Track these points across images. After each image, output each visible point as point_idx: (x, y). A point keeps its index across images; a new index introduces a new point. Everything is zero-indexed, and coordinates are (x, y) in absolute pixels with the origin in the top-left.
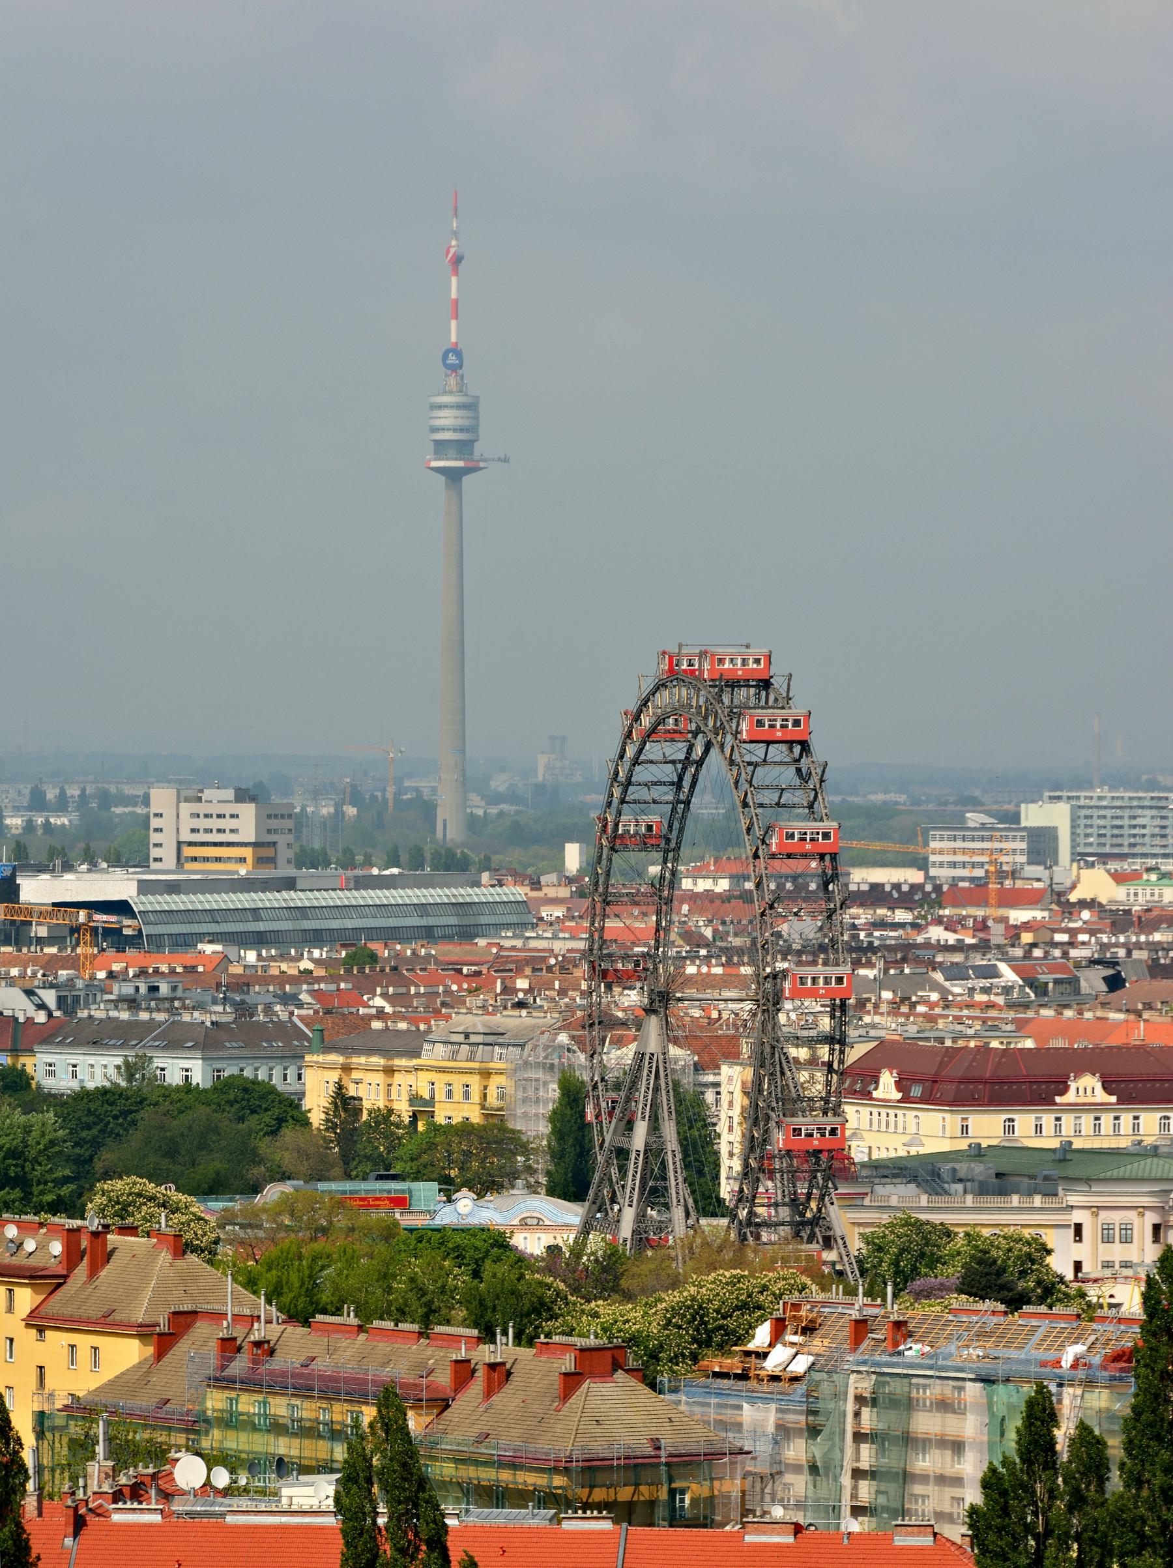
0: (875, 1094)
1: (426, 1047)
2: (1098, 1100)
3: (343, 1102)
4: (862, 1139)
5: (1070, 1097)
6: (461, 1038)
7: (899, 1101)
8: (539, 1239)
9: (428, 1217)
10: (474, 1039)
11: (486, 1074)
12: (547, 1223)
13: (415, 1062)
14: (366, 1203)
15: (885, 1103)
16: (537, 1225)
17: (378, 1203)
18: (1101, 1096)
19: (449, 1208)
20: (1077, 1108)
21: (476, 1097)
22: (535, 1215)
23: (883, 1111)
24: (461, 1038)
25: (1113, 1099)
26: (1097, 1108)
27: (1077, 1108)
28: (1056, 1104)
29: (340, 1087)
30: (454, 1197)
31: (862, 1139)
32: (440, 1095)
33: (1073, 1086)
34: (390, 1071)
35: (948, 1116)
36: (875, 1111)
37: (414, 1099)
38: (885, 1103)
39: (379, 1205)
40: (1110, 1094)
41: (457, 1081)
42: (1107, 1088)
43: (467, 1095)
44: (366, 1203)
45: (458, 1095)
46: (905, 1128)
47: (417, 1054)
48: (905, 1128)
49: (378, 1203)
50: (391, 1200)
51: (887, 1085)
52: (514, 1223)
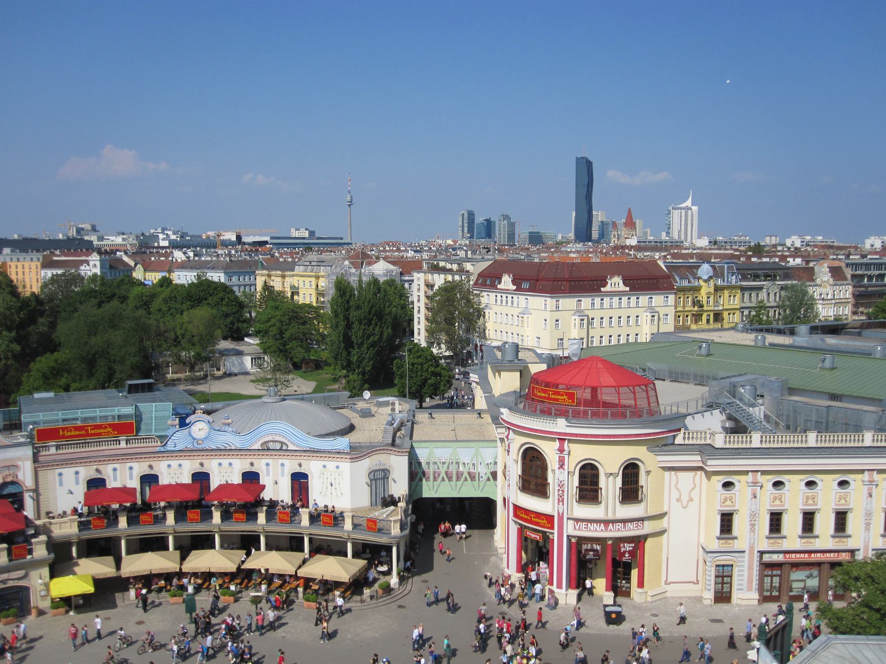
0: (499, 286)
1: (297, 267)
2: (621, 289)
3: (267, 287)
4: (491, 309)
5: (608, 288)
6: (308, 263)
7: (515, 290)
8: (283, 465)
9: (159, 443)
10: (313, 264)
11: (318, 278)
12: (291, 447)
13: (292, 273)
14: (83, 432)
15: (506, 291)
16: (281, 449)
17: (98, 431)
18: (622, 288)
19: (184, 432)
20: (612, 294)
21: (314, 286)
22: (277, 438)
23: (504, 296)
24: (308, 263)
25: (628, 289)
26: (620, 294)
27: (612, 294)
28: (601, 292)
29: (265, 282)
30: (187, 421)
31: (491, 309)
32: (301, 286)
33: (609, 282)
34: (284, 277)
35: (548, 299)
36: (499, 295)
37: (292, 287)
38: (506, 291)
39: (100, 434)
40: (626, 286)
41: (307, 280)
42: (625, 284)
43: (311, 285)
44: (83, 432)
45: (307, 285)
46: (518, 304)
47: (293, 270)
48: (518, 304)
49: (98, 431)
50: (114, 426)
51: (507, 282)
52: (255, 447)
